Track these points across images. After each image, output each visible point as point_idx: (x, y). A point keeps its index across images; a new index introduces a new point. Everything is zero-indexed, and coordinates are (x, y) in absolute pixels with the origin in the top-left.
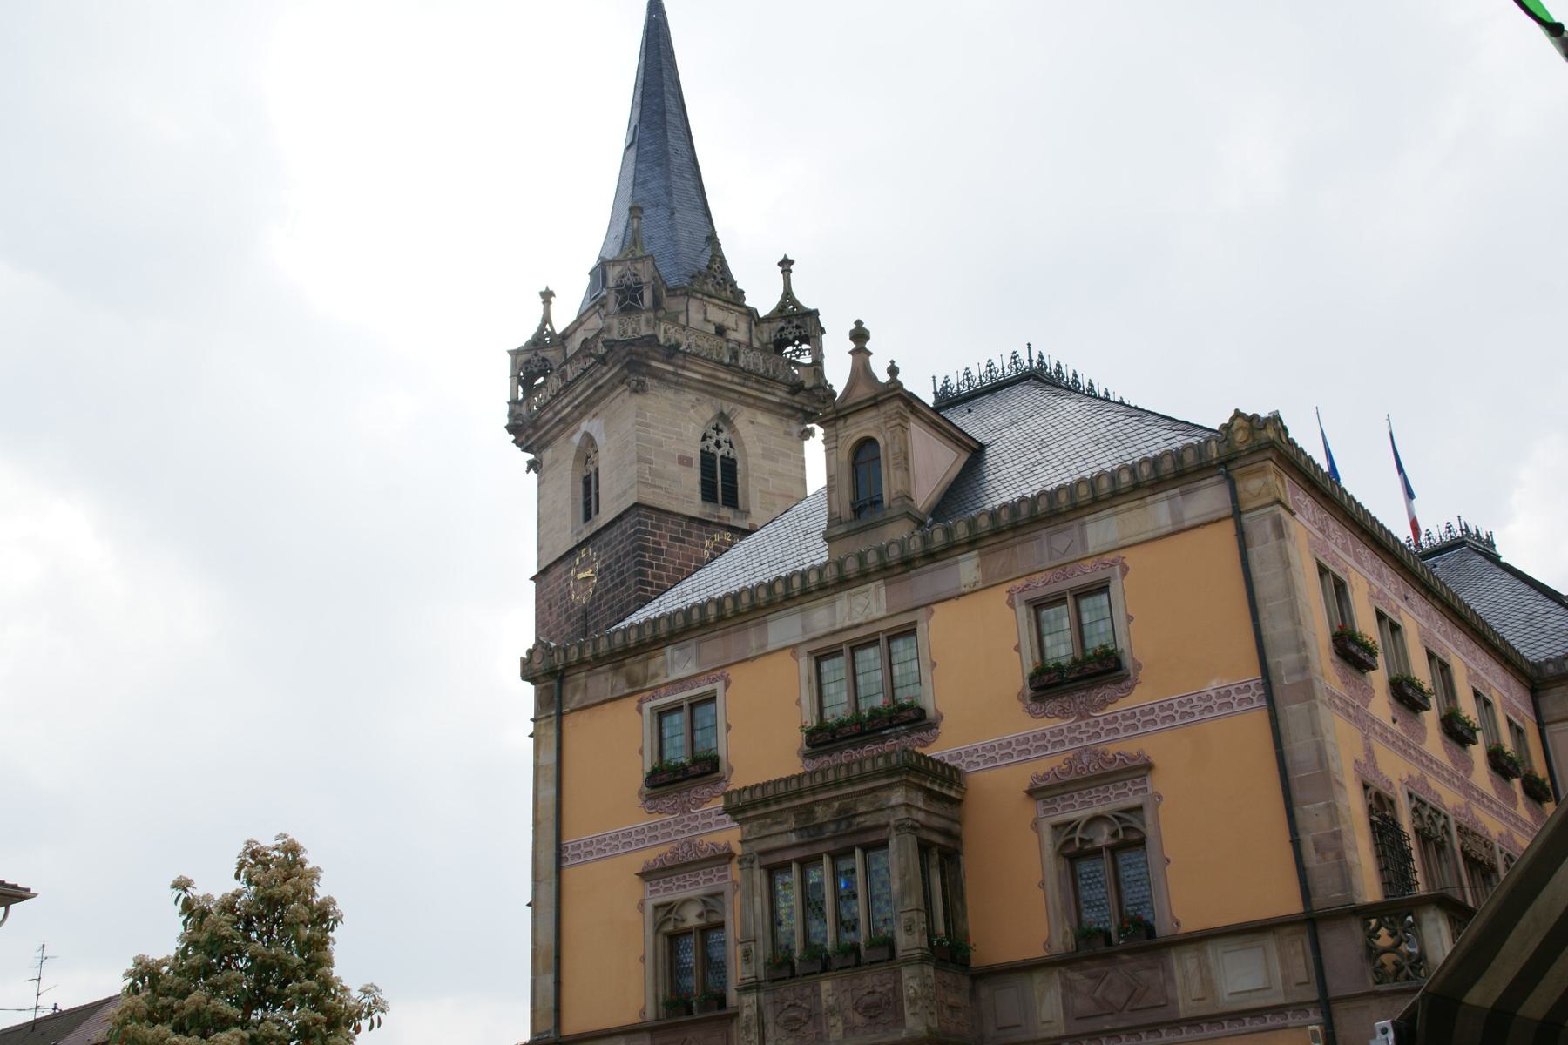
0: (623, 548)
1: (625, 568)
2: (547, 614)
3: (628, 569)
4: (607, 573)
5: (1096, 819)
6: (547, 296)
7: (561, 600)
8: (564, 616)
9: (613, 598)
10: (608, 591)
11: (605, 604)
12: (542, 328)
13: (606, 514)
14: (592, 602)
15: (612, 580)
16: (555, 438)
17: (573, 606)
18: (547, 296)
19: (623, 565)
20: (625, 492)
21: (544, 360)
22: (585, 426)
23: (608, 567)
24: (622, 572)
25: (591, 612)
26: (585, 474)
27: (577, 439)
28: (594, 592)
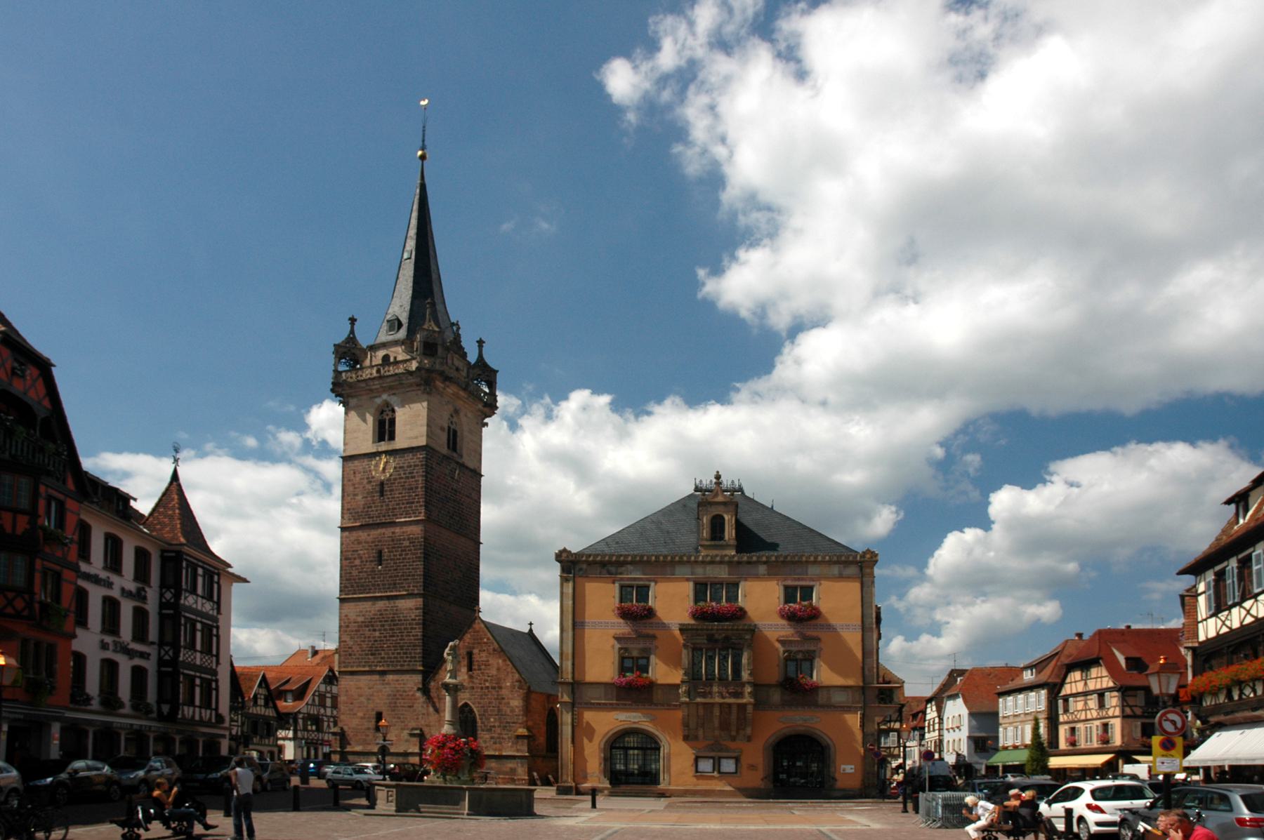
0: (414, 462)
1: (415, 471)
2: (352, 476)
3: (417, 473)
4: (401, 470)
5: (799, 651)
6: (353, 321)
7: (364, 472)
8: (366, 481)
9: (405, 482)
10: (402, 478)
11: (399, 483)
12: (349, 335)
13: (400, 442)
14: (389, 480)
15: (405, 474)
16: (360, 395)
17: (373, 477)
18: (353, 321)
19: (414, 469)
20: (416, 437)
21: (354, 354)
22: (385, 397)
23: (400, 467)
24: (413, 473)
25: (387, 484)
26: (380, 418)
27: (378, 401)
28: (391, 476)
